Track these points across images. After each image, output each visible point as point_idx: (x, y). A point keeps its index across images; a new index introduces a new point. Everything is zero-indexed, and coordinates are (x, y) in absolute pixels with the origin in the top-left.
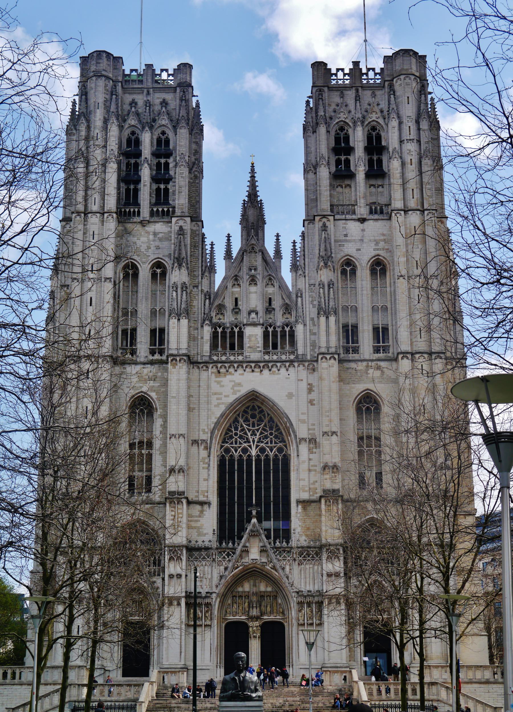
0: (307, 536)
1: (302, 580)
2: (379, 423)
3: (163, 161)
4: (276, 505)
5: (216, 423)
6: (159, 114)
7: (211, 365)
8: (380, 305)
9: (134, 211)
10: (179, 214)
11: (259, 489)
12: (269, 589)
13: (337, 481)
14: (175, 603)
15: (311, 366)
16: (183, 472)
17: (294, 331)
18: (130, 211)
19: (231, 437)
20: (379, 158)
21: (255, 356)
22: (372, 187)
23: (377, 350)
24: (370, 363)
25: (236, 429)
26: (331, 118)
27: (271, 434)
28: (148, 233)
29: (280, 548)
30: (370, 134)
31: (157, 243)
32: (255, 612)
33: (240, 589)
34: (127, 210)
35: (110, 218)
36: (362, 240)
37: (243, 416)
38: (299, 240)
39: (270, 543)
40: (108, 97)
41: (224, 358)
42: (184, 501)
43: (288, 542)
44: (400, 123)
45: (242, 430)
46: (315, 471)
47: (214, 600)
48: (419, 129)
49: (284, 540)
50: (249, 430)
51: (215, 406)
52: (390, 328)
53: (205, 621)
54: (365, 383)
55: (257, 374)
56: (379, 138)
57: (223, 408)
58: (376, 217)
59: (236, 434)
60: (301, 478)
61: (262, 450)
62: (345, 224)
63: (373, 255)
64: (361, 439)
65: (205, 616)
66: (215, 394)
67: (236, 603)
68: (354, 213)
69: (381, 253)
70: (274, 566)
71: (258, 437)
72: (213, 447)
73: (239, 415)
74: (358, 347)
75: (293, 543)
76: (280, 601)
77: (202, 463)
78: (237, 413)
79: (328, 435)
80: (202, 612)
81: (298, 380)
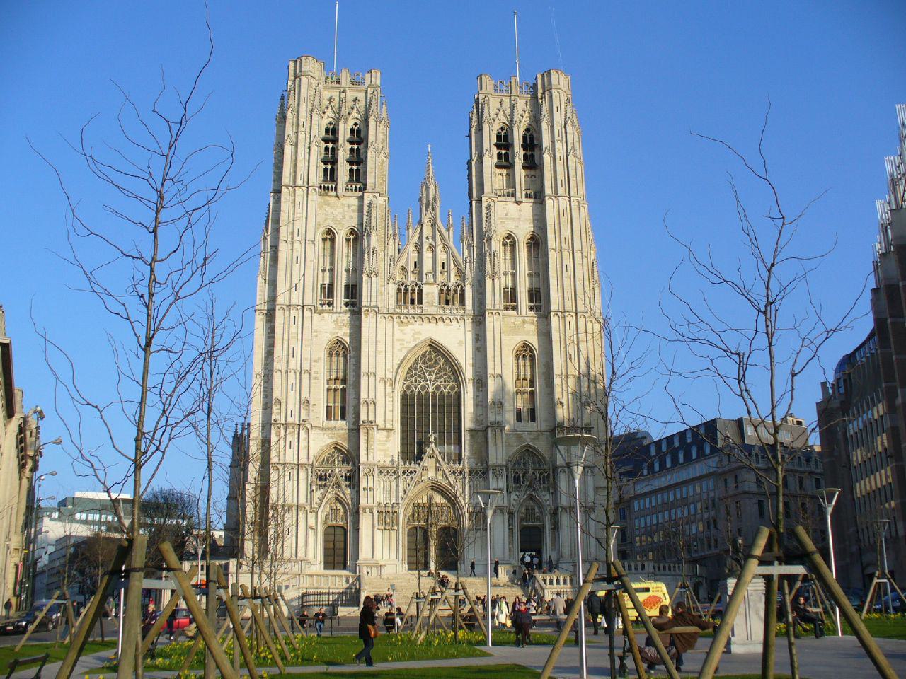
3: (356, 147)
4: (449, 432)
5: (399, 367)
6: (353, 109)
7: (395, 316)
9: (332, 187)
10: (370, 191)
14: (368, 510)
15: (478, 320)
16: (375, 403)
18: (328, 187)
19: (412, 376)
20: (532, 154)
21: (432, 310)
23: (531, 309)
24: (526, 318)
25: (416, 370)
27: (445, 375)
28: (343, 205)
31: (350, 214)
33: (420, 501)
34: (326, 186)
35: (313, 191)
36: (519, 219)
40: (313, 93)
41: (405, 311)
43: (460, 463)
44: (552, 127)
45: (421, 371)
46: (482, 405)
48: (566, 133)
50: (427, 371)
51: (399, 350)
52: (541, 291)
54: (523, 335)
55: (433, 325)
56: (532, 138)
57: (405, 352)
58: (532, 200)
59: (416, 374)
61: (438, 388)
64: (518, 379)
65: (393, 523)
66: (399, 340)
68: (513, 195)
71: (434, 377)
72: (397, 382)
73: (418, 358)
74: (517, 306)
78: (417, 356)
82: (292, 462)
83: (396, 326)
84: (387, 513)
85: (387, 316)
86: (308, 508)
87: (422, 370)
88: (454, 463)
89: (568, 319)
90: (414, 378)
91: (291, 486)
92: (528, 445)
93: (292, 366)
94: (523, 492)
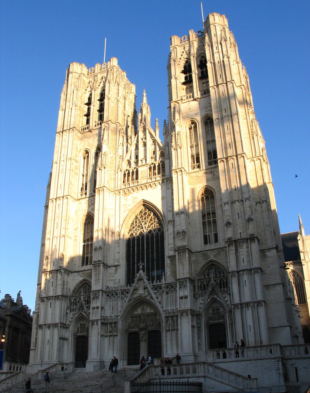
0: (173, 277)
1: (169, 304)
2: (214, 204)
4: (158, 261)
7: (121, 191)
8: (210, 139)
11: (148, 254)
12: (152, 311)
13: (185, 240)
14: (95, 323)
16: (101, 249)
17: (164, 164)
19: (134, 227)
21: (144, 181)
22: (204, 84)
26: (180, 59)
27: (154, 222)
28: (93, 135)
29: (155, 285)
30: (201, 60)
32: (142, 325)
33: (136, 313)
37: (140, 214)
38: (167, 119)
39: (149, 283)
42: (101, 265)
43: (160, 282)
47: (118, 320)
49: (158, 281)
50: (143, 222)
53: (114, 333)
55: (145, 191)
57: (127, 212)
60: (169, 243)
62: (189, 103)
63: (205, 114)
65: (114, 330)
67: (133, 321)
68: (193, 96)
69: (209, 112)
70: (152, 296)
71: (148, 224)
74: (200, 164)
75: (163, 281)
76: (158, 318)
77: (117, 244)
79: (179, 214)
80: (112, 328)
81: (167, 189)
82: (53, 295)
83: (122, 197)
84: (111, 323)
85: (116, 192)
86: (59, 325)
87: (140, 222)
88: (157, 282)
89: (231, 161)
90: (135, 228)
91: (50, 310)
92: (212, 261)
93: (55, 234)
94: (207, 297)
